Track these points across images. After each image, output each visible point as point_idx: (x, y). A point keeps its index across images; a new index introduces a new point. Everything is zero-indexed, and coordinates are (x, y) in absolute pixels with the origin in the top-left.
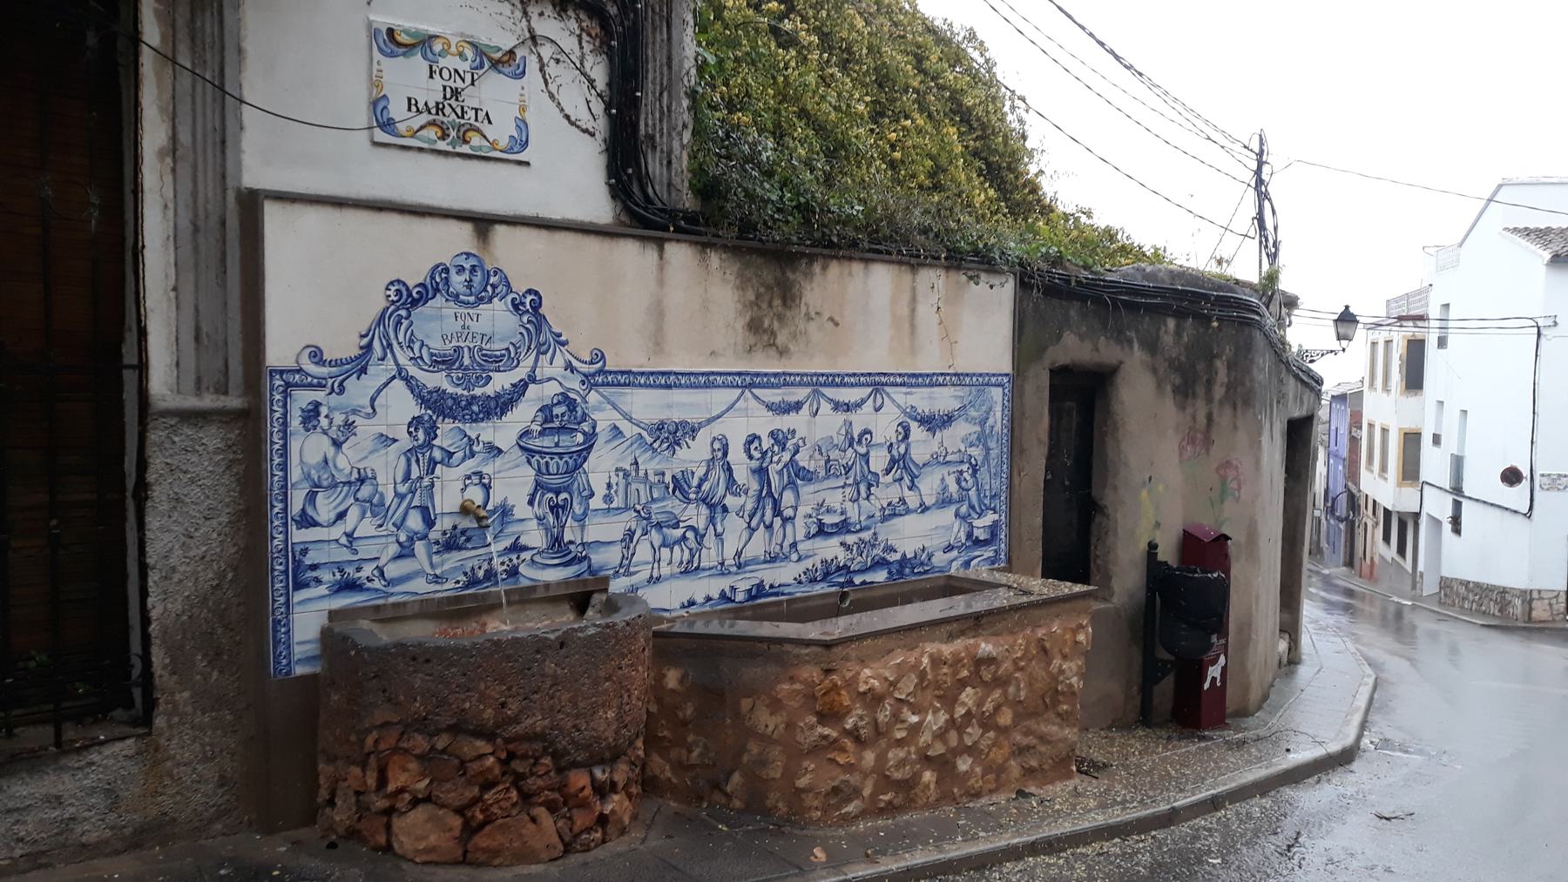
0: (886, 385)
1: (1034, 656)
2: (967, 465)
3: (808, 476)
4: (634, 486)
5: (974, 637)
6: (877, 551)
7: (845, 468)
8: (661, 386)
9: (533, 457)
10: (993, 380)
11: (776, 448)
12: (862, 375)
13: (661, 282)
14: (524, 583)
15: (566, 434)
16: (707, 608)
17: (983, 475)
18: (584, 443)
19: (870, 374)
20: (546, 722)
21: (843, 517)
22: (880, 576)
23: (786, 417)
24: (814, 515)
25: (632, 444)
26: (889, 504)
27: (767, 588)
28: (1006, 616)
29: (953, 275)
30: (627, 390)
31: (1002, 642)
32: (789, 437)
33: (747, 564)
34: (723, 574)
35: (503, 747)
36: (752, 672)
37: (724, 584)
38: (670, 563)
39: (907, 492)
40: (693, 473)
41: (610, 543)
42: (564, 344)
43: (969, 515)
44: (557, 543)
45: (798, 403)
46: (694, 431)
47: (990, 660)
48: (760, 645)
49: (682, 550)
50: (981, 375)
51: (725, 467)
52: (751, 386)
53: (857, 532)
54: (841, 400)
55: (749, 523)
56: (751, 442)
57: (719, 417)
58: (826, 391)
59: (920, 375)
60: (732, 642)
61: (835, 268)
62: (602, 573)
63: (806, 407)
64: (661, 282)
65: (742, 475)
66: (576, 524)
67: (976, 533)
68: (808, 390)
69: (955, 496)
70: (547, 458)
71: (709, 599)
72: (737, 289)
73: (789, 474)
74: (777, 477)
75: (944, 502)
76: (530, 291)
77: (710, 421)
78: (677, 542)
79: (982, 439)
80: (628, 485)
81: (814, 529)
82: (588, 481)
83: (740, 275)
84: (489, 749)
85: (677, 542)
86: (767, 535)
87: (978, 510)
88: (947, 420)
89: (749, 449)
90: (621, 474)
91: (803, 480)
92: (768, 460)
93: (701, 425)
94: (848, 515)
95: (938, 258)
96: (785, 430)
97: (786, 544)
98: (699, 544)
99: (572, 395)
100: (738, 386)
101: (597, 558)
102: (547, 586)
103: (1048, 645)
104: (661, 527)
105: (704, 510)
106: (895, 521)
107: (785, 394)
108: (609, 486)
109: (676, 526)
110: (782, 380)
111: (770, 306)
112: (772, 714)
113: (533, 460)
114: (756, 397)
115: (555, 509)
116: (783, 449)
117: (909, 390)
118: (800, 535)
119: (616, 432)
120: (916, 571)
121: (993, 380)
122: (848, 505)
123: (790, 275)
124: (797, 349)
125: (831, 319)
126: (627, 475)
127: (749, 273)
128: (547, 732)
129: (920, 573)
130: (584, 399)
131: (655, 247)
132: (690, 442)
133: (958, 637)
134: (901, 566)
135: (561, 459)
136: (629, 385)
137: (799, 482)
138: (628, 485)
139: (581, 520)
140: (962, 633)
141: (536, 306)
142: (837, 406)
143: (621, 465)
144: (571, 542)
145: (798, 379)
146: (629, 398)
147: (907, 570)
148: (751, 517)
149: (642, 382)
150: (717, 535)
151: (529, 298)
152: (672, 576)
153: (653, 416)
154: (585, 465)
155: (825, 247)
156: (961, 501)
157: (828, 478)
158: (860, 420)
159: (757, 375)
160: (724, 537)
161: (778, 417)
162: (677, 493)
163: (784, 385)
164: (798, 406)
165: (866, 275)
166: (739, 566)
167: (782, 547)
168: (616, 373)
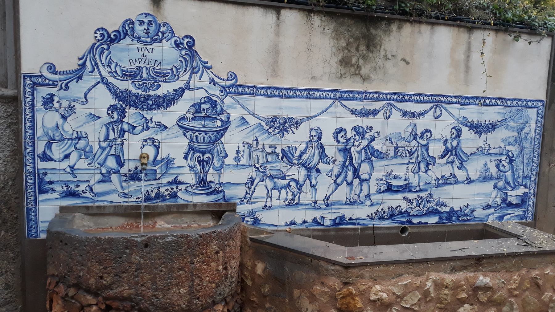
0: (445, 102)
1: (527, 289)
2: (505, 157)
3: (381, 156)
4: (255, 153)
5: (475, 271)
6: (432, 205)
7: (409, 152)
8: (275, 96)
9: (187, 132)
10: (530, 104)
11: (357, 137)
12: (426, 95)
13: (277, 34)
14: (181, 202)
15: (210, 120)
16: (304, 227)
17: (518, 164)
18: (222, 126)
19: (432, 95)
20: (132, 291)
21: (407, 182)
22: (434, 220)
23: (365, 119)
24: (384, 179)
25: (254, 129)
26: (443, 177)
27: (347, 219)
28: (504, 260)
29: (501, 36)
30: (252, 97)
31: (499, 277)
32: (368, 131)
33: (332, 204)
34: (315, 209)
35: (102, 302)
36: (300, 274)
37: (317, 214)
38: (279, 199)
39: (456, 171)
40: (296, 148)
41: (238, 184)
42: (211, 68)
43: (505, 188)
44: (203, 182)
45: (375, 110)
46: (297, 124)
47: (486, 288)
48: (307, 258)
49: (287, 192)
50: (520, 100)
51: (319, 147)
52: (340, 99)
53: (417, 192)
54: (409, 110)
55: (335, 181)
56: (339, 132)
57: (316, 116)
58: (396, 104)
59: (472, 98)
60: (291, 253)
61: (407, 29)
62: (232, 201)
63: (381, 114)
64: (277, 34)
65: (331, 149)
66: (215, 172)
67: (509, 199)
68: (384, 103)
69: (494, 175)
70: (197, 134)
71: (305, 222)
72: (333, 39)
73: (366, 154)
74: (357, 155)
75: (485, 178)
76: (186, 36)
77: (309, 118)
78: (284, 187)
79: (519, 141)
80: (251, 152)
81: (383, 188)
82: (224, 148)
83: (335, 30)
84: (94, 301)
85: (284, 187)
86: (348, 189)
87: (512, 185)
88: (492, 127)
89: (337, 137)
90: (246, 146)
91: (377, 157)
92: (351, 144)
93: (302, 121)
94: (411, 181)
95: (490, 24)
96: (364, 126)
97: (362, 195)
98: (299, 190)
99: (213, 98)
100: (330, 99)
101: (229, 192)
102: (195, 205)
103: (541, 282)
104: (273, 178)
105: (303, 171)
106: (447, 187)
107: (365, 105)
108: (238, 152)
109: (284, 178)
110: (365, 96)
111: (357, 49)
112: (310, 303)
113: (187, 134)
114: (344, 106)
115: (201, 162)
116: (363, 138)
117: (462, 107)
118: (373, 190)
119: (244, 121)
120: (460, 219)
121: (530, 104)
122: (411, 175)
123: (373, 31)
124: (376, 77)
125: (404, 60)
126: (250, 146)
127: (342, 29)
128: (133, 296)
129: (464, 220)
130: (222, 101)
131: (274, 12)
132: (295, 130)
133: (461, 270)
134: (449, 215)
135: (206, 134)
136: (253, 94)
137: (373, 158)
138: (251, 152)
139: (219, 170)
140: (464, 268)
141: (191, 45)
142: (405, 114)
143: (246, 140)
144: (212, 182)
145: (376, 96)
146: (252, 102)
147: (454, 218)
148: (337, 177)
149: (262, 93)
150: (312, 186)
151: (186, 40)
152: (280, 207)
153: (271, 113)
154: (222, 139)
155: (399, 14)
156: (499, 178)
157: (396, 158)
158: (421, 124)
159: (346, 92)
160: (317, 187)
161: (360, 119)
162: (285, 159)
163: (365, 99)
164: (375, 113)
165: (432, 33)
166: (327, 205)
167: (359, 196)
168: (244, 86)
